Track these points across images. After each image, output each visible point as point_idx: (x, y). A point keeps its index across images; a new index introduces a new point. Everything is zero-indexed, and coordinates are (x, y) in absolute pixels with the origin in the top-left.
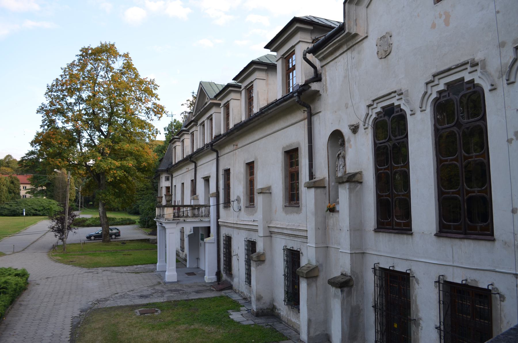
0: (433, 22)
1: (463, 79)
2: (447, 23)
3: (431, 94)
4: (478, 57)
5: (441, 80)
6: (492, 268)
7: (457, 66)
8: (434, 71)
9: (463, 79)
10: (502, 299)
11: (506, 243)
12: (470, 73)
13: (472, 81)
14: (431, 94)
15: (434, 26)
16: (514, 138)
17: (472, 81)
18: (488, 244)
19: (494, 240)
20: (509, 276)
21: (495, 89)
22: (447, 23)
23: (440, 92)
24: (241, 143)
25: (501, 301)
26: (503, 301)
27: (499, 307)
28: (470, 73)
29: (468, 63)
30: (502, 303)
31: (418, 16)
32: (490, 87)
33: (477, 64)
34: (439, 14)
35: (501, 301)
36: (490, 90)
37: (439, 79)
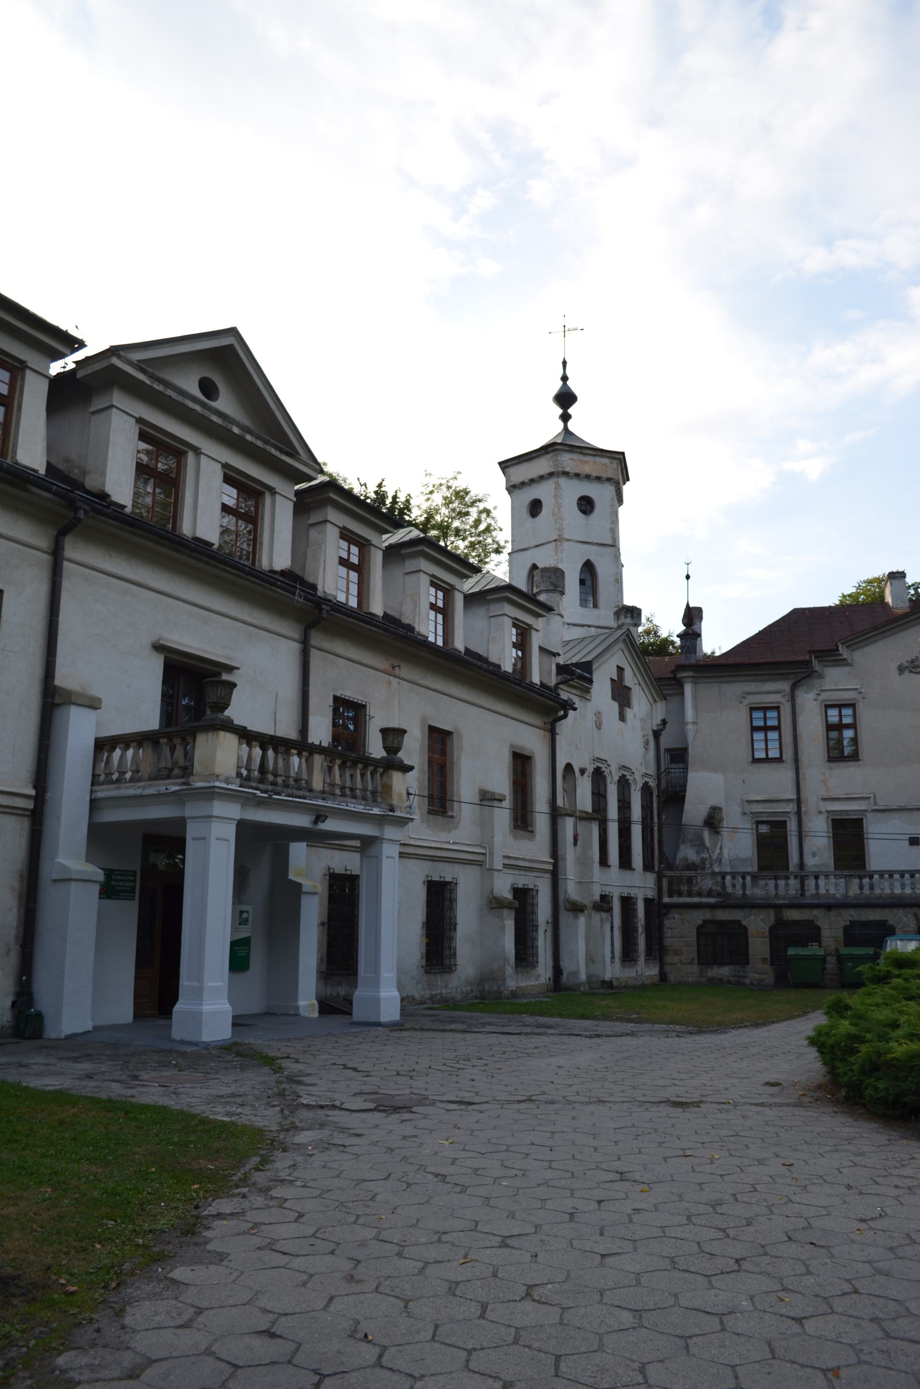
24: (406, 671)
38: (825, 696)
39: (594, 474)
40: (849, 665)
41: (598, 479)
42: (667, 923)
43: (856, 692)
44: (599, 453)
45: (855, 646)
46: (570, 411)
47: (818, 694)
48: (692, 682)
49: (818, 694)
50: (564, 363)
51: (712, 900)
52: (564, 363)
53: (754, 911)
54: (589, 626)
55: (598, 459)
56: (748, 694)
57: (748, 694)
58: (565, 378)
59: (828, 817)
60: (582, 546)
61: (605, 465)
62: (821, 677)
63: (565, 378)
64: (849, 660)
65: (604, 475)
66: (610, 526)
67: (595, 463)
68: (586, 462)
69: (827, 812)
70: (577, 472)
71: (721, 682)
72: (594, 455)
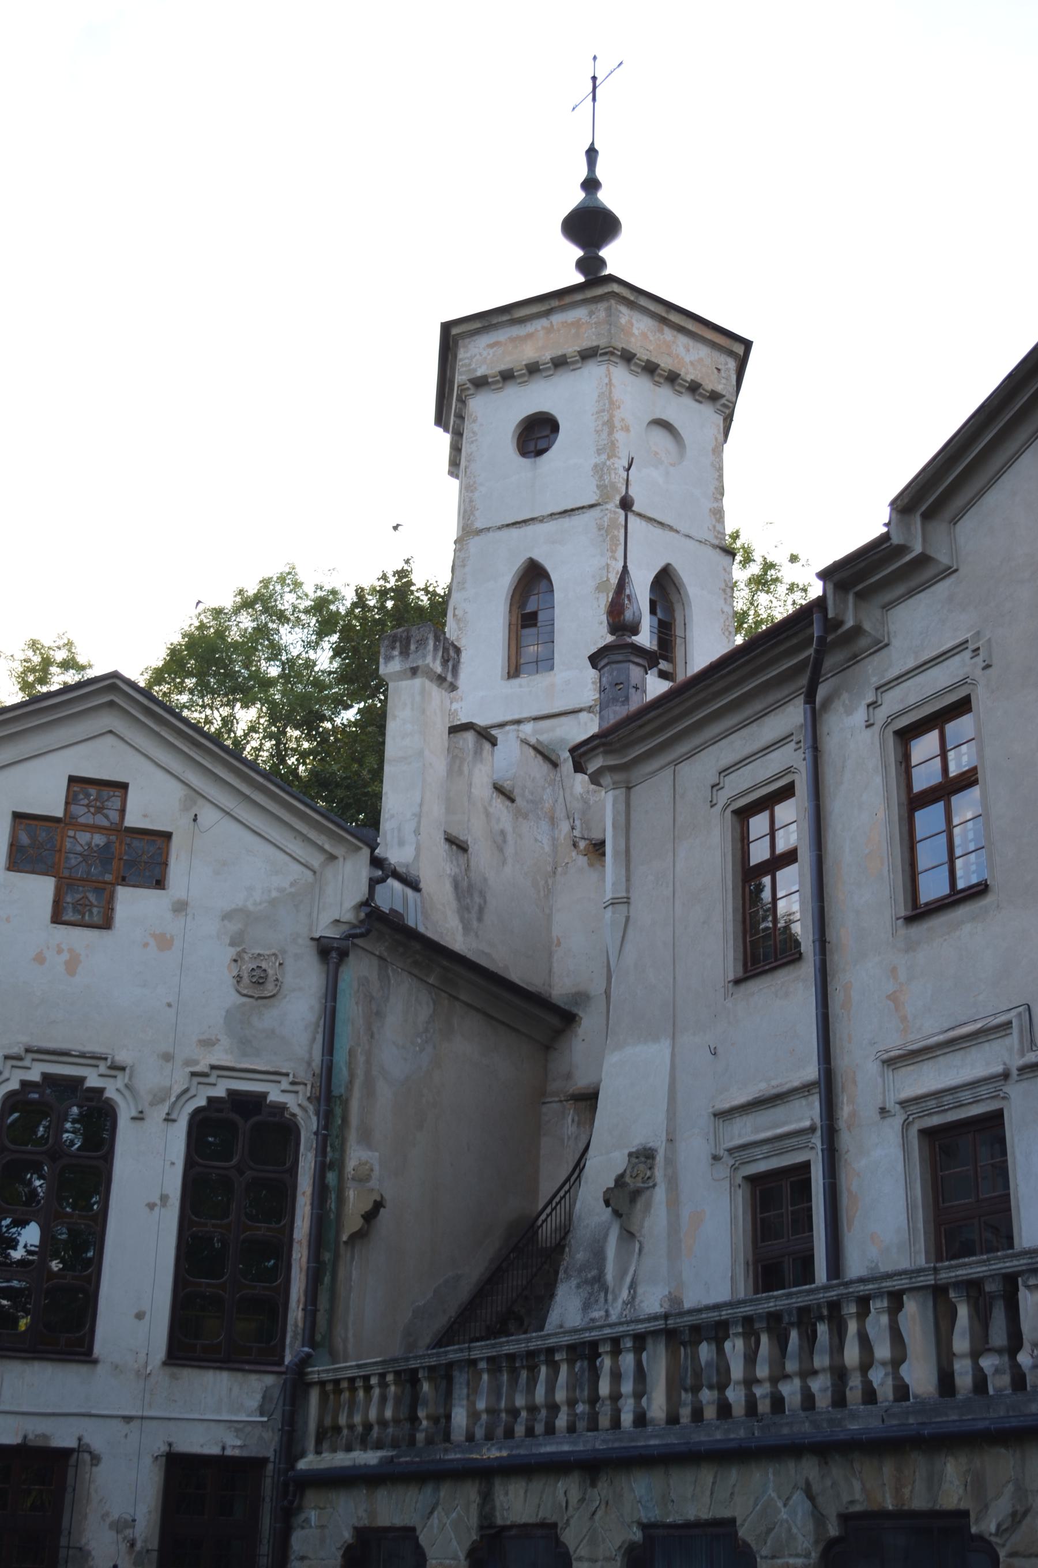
0: (41, 953)
1: (83, 1079)
2: (72, 966)
3: (8, 1080)
4: (122, 1057)
5: (36, 1064)
6: (83, 1411)
7: (83, 1055)
8: (25, 1039)
9: (83, 1079)
10: (94, 1462)
11: (117, 1367)
12: (101, 1075)
13: (101, 1091)
14: (8, 1080)
15: (40, 959)
16: (158, 1202)
17: (101, 1091)
18: (84, 1369)
19: (95, 1362)
20: (114, 1421)
21: (142, 1119)
22: (72, 966)
23: (24, 1084)
25: (92, 1465)
26: (96, 1465)
27: (87, 1476)
28: (101, 1075)
29: (106, 1059)
30: (94, 1469)
31: (8, 920)
32: (134, 1114)
33: (123, 1069)
34: (58, 945)
35: (92, 1465)
36: (133, 1118)
37: (33, 1060)
38: (893, 701)
39: (547, 356)
40: (949, 572)
41: (560, 363)
42: (298, 1541)
43: (967, 654)
44: (555, 303)
45: (959, 502)
46: (603, 253)
47: (873, 705)
48: (616, 786)
49: (873, 705)
50: (592, 154)
51: (369, 1458)
52: (592, 154)
53: (445, 1490)
54: (518, 722)
55: (557, 319)
56: (725, 771)
57: (725, 771)
58: (591, 185)
59: (906, 1125)
60: (514, 532)
61: (577, 324)
62: (881, 645)
63: (591, 185)
64: (943, 558)
65: (571, 348)
66: (594, 460)
67: (549, 330)
68: (530, 336)
69: (904, 1104)
70: (503, 367)
71: (677, 762)
72: (548, 313)
